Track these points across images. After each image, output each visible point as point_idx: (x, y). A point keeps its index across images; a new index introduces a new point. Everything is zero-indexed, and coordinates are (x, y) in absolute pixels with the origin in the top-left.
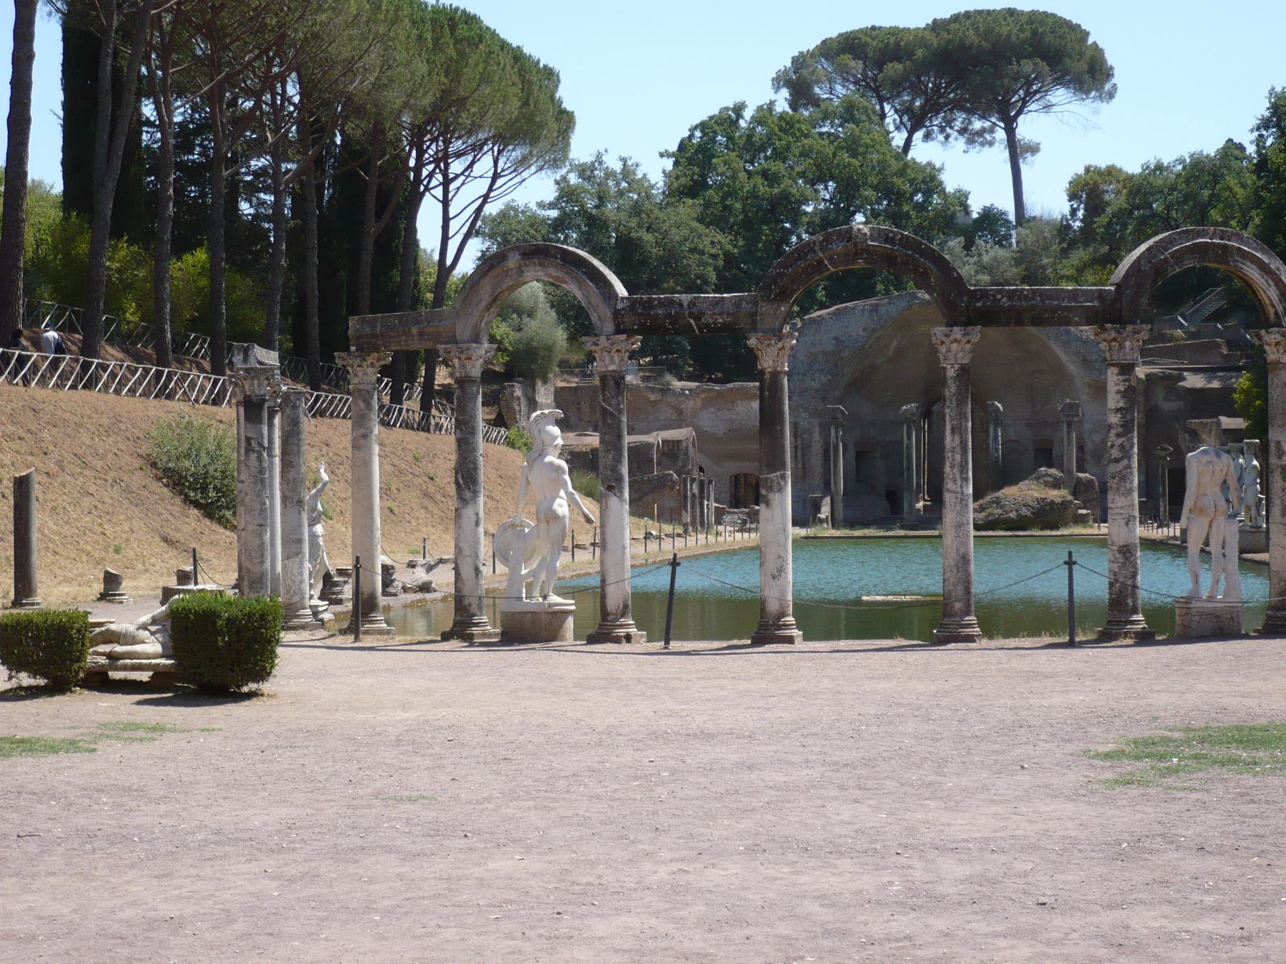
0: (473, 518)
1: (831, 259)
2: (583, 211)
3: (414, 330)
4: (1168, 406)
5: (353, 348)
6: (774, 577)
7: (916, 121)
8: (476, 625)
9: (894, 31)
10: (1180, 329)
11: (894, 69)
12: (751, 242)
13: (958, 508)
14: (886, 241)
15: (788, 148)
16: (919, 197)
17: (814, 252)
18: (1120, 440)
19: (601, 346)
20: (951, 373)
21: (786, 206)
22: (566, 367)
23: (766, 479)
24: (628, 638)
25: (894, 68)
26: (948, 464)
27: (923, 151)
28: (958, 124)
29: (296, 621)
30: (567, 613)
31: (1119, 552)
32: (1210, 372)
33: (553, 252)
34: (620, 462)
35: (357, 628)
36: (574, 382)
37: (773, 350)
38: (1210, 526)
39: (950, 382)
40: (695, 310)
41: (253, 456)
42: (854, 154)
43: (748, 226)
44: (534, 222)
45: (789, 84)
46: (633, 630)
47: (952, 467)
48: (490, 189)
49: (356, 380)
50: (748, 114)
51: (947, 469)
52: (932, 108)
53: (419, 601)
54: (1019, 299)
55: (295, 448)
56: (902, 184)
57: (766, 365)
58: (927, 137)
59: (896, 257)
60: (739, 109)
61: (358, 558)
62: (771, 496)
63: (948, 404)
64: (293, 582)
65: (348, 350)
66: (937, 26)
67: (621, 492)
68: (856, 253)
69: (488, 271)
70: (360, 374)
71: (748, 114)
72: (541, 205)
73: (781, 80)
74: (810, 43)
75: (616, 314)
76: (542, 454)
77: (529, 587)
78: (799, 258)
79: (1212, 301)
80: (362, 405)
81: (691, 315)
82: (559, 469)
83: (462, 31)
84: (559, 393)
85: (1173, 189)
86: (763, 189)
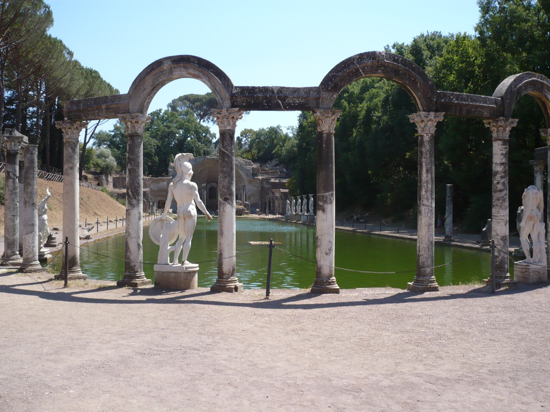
0: (137, 215)
1: (363, 69)
2: (121, 133)
3: (104, 107)
4: (266, 186)
5: (66, 119)
6: (327, 254)
7: (202, 117)
8: (138, 277)
9: (197, 95)
10: (268, 167)
11: (198, 104)
12: (163, 142)
13: (429, 215)
14: (394, 61)
15: (172, 120)
16: (204, 134)
17: (354, 64)
18: (503, 180)
19: (223, 115)
20: (426, 138)
21: (171, 134)
22: (117, 173)
23: (323, 196)
24: (236, 289)
25: (198, 104)
26: (424, 190)
27: (204, 124)
28: (211, 119)
29: (30, 268)
30: (194, 272)
31: (501, 239)
32: (276, 178)
33: (192, 60)
34: (232, 184)
35: (66, 275)
36: (118, 176)
37: (328, 121)
38: (533, 226)
39: (426, 144)
40: (281, 95)
41: (11, 181)
42: (189, 122)
43: (161, 139)
44: (108, 135)
45: (171, 106)
46: (238, 284)
47: (426, 191)
49: (67, 137)
50: (163, 112)
51: (423, 193)
53: (86, 243)
54: (461, 100)
55: (32, 176)
56: (201, 131)
57: (324, 129)
58: (204, 121)
59: (400, 71)
60: (160, 110)
61: (67, 238)
62: (326, 206)
63: (424, 156)
64: (30, 247)
65: (63, 120)
67: (232, 202)
68: (378, 67)
69: (150, 72)
70: (69, 133)
71: (163, 112)
72: (109, 131)
73: (169, 105)
74: (177, 97)
75: (232, 96)
76: (182, 179)
77: (172, 255)
78: (345, 67)
79: (274, 162)
80: (70, 150)
81: (279, 98)
82: (192, 188)
83: (94, 74)
84: (114, 179)
85: (266, 134)
86: (166, 130)
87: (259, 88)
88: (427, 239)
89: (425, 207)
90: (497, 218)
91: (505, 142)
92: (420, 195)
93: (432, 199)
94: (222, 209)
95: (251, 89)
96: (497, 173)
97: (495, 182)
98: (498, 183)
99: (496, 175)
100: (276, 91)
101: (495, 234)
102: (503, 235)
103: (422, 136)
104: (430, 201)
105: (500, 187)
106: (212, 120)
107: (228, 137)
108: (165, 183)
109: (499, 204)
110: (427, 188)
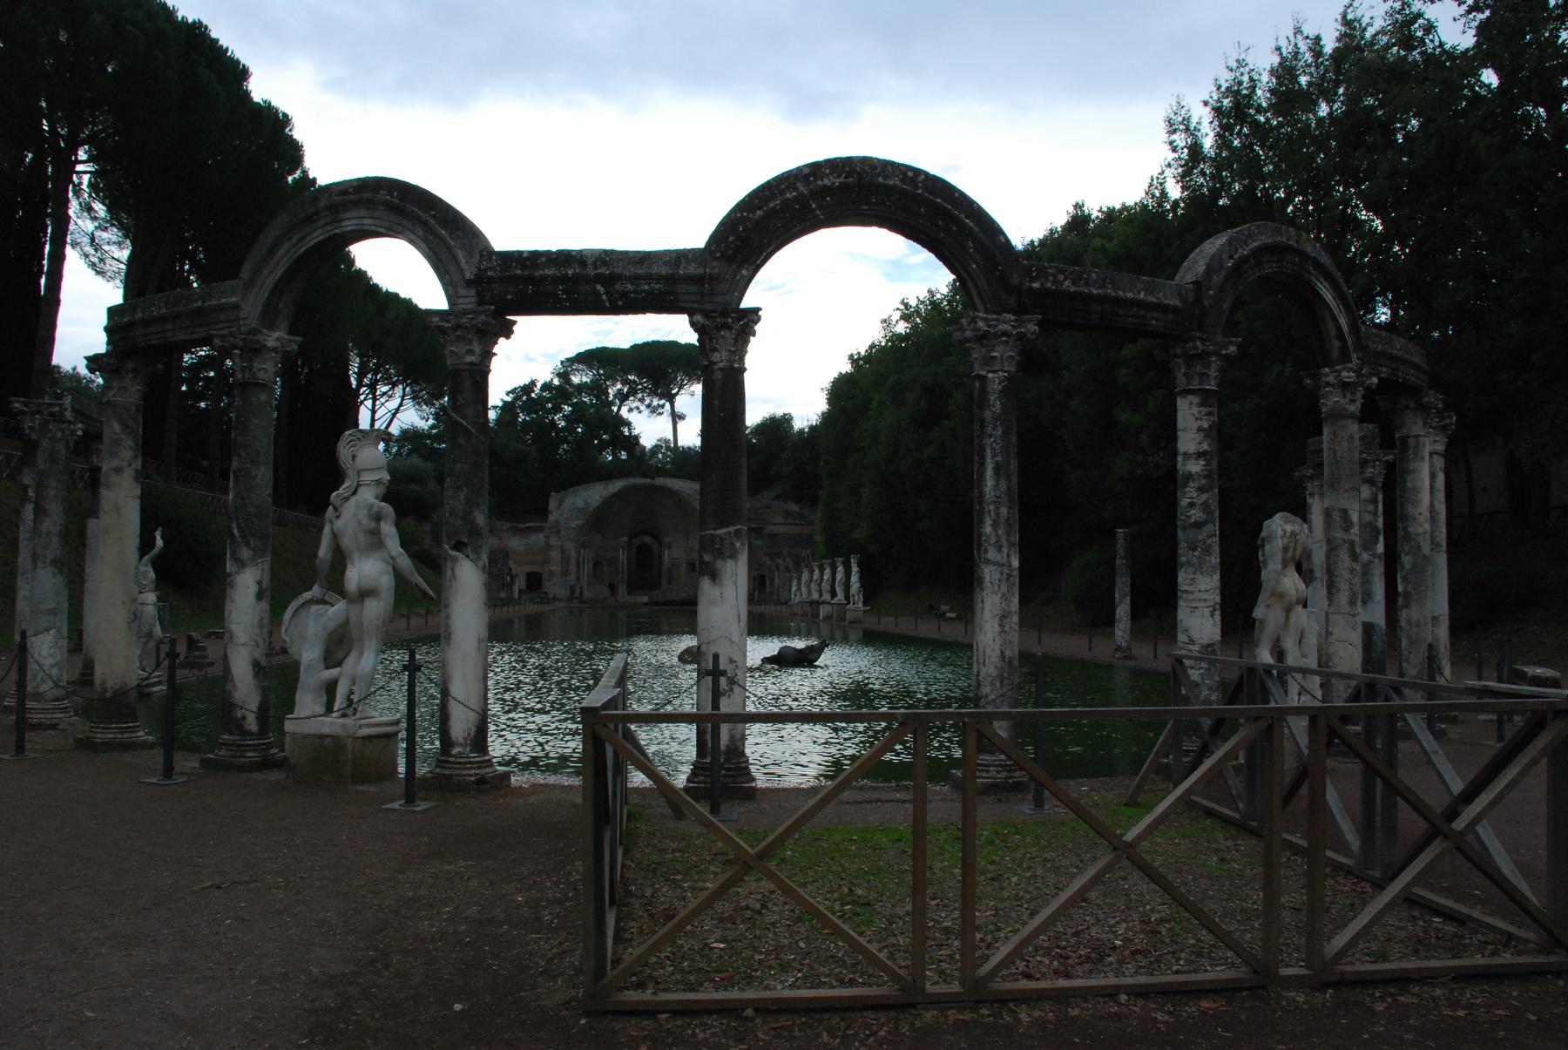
7: (623, 398)
13: (1004, 588)
18: (1204, 497)
26: (988, 522)
45: (559, 375)
47: (995, 525)
48: (401, 405)
50: (539, 385)
52: (633, 392)
60: (533, 383)
62: (719, 564)
63: (989, 430)
66: (635, 347)
87: (548, 254)
88: (997, 652)
89: (992, 568)
90: (1191, 597)
91: (1206, 397)
92: (980, 535)
93: (1011, 545)
94: (449, 574)
95: (527, 259)
96: (1189, 477)
97: (1185, 502)
98: (1192, 505)
99: (1185, 485)
100: (590, 261)
101: (1186, 639)
102: (1205, 642)
103: (983, 378)
104: (1005, 550)
105: (1196, 515)
106: (648, 406)
107: (467, 384)
108: (541, 535)
109: (1195, 560)
110: (998, 515)
